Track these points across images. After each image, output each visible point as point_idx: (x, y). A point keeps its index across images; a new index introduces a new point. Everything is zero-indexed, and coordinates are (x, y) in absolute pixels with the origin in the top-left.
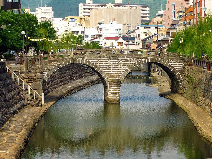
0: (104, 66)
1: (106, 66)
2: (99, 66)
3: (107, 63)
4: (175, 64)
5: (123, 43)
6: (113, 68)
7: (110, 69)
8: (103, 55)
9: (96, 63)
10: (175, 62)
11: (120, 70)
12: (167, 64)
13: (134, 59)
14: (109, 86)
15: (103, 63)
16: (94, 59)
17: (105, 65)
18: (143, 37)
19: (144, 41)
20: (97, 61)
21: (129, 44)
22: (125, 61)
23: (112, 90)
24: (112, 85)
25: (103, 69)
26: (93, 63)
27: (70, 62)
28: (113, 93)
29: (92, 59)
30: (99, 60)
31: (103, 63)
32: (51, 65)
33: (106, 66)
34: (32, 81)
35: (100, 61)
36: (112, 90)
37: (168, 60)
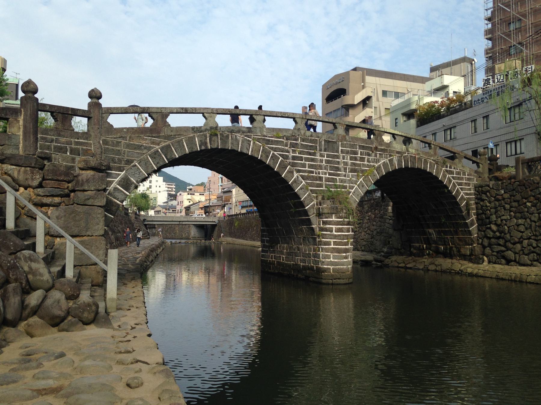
0: (304, 166)
1: (310, 166)
2: (294, 165)
3: (313, 160)
4: (459, 178)
5: (162, 212)
6: (327, 176)
7: (321, 179)
8: (303, 132)
9: (282, 156)
10: (458, 173)
11: (345, 182)
12: (444, 176)
13: (376, 156)
14: (326, 230)
15: (301, 159)
16: (277, 143)
17: (307, 163)
18: (186, 204)
19: (188, 209)
20: (287, 148)
21: (169, 213)
22: (356, 159)
23: (335, 243)
24: (334, 227)
25: (303, 177)
26: (275, 153)
27: (206, 143)
28: (339, 251)
29: (273, 142)
30: (293, 145)
31: (301, 159)
32: (139, 147)
33: (310, 166)
34: (57, 200)
35: (294, 151)
36: (335, 243)
37: (447, 167)
